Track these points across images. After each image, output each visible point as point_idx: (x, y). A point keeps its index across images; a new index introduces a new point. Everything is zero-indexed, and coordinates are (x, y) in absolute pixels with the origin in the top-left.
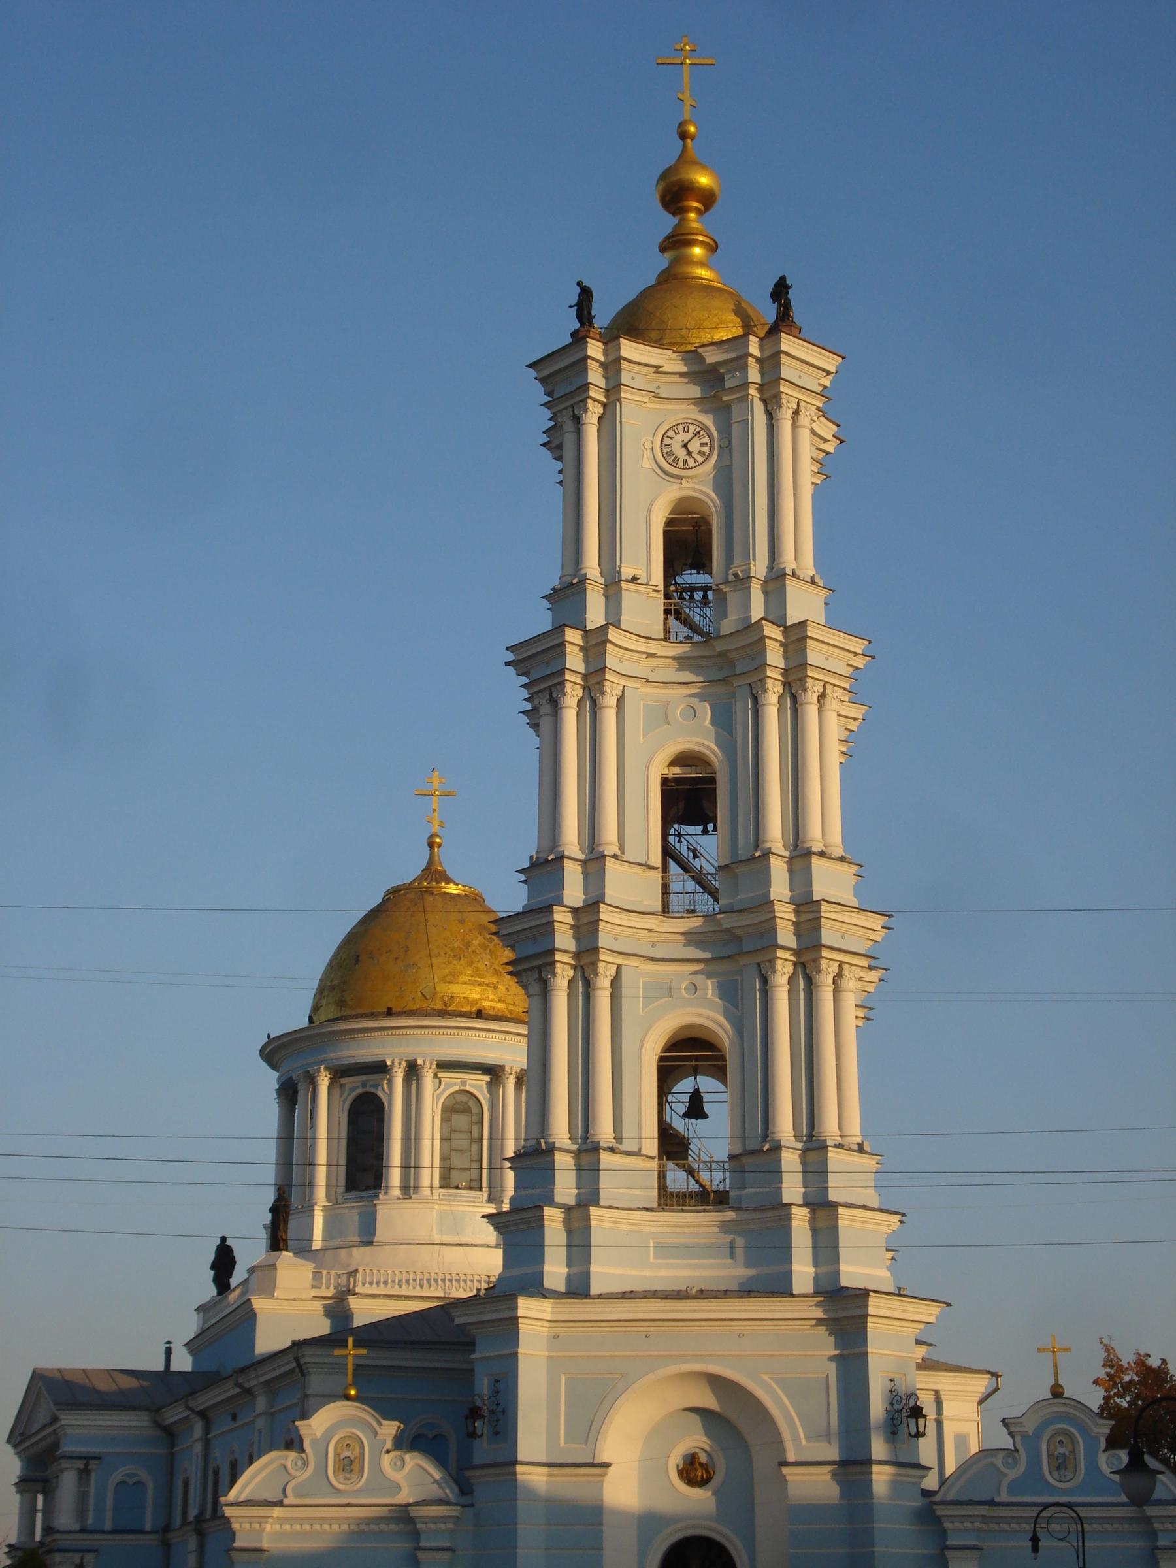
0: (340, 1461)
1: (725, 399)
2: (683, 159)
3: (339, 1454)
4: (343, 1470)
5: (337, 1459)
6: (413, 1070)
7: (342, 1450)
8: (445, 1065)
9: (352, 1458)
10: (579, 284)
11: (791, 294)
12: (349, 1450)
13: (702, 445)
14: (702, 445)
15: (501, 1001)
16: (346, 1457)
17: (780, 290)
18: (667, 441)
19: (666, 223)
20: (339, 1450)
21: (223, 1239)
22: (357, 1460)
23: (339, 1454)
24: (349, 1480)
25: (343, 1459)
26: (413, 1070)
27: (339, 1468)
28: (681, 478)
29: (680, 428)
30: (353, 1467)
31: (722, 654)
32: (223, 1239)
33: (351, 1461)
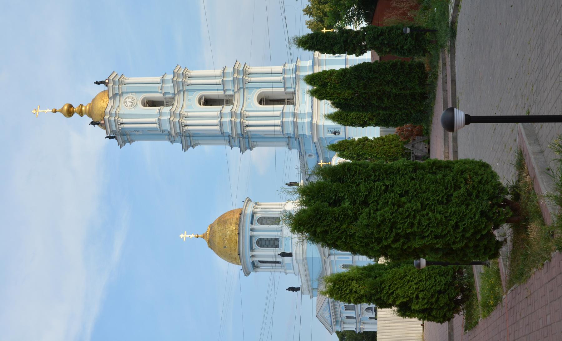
1: (121, 93)
2: (61, 111)
6: (252, 230)
8: (252, 223)
10: (90, 124)
11: (98, 81)
13: (130, 99)
14: (130, 99)
15: (237, 214)
17: (97, 83)
18: (128, 106)
19: (76, 115)
21: (287, 290)
26: (252, 230)
28: (137, 103)
29: (126, 103)
31: (178, 92)
32: (287, 290)
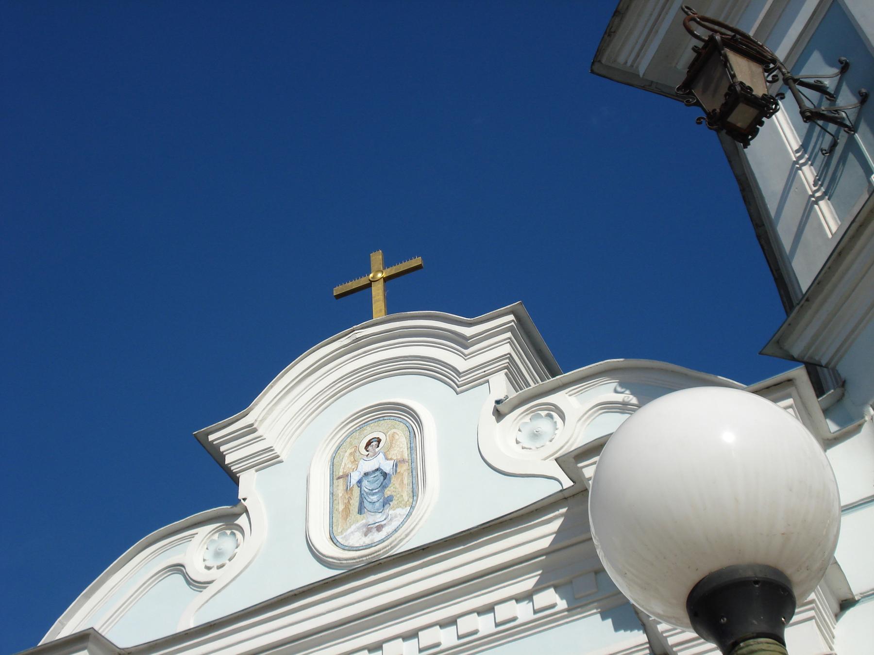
0: (348, 490)
3: (346, 476)
4: (360, 511)
5: (340, 491)
7: (355, 461)
9: (387, 467)
12: (375, 455)
16: (366, 474)
20: (345, 464)
22: (403, 468)
23: (346, 476)
24: (379, 528)
25: (360, 482)
27: (347, 509)
30: (388, 492)
33: (385, 475)
